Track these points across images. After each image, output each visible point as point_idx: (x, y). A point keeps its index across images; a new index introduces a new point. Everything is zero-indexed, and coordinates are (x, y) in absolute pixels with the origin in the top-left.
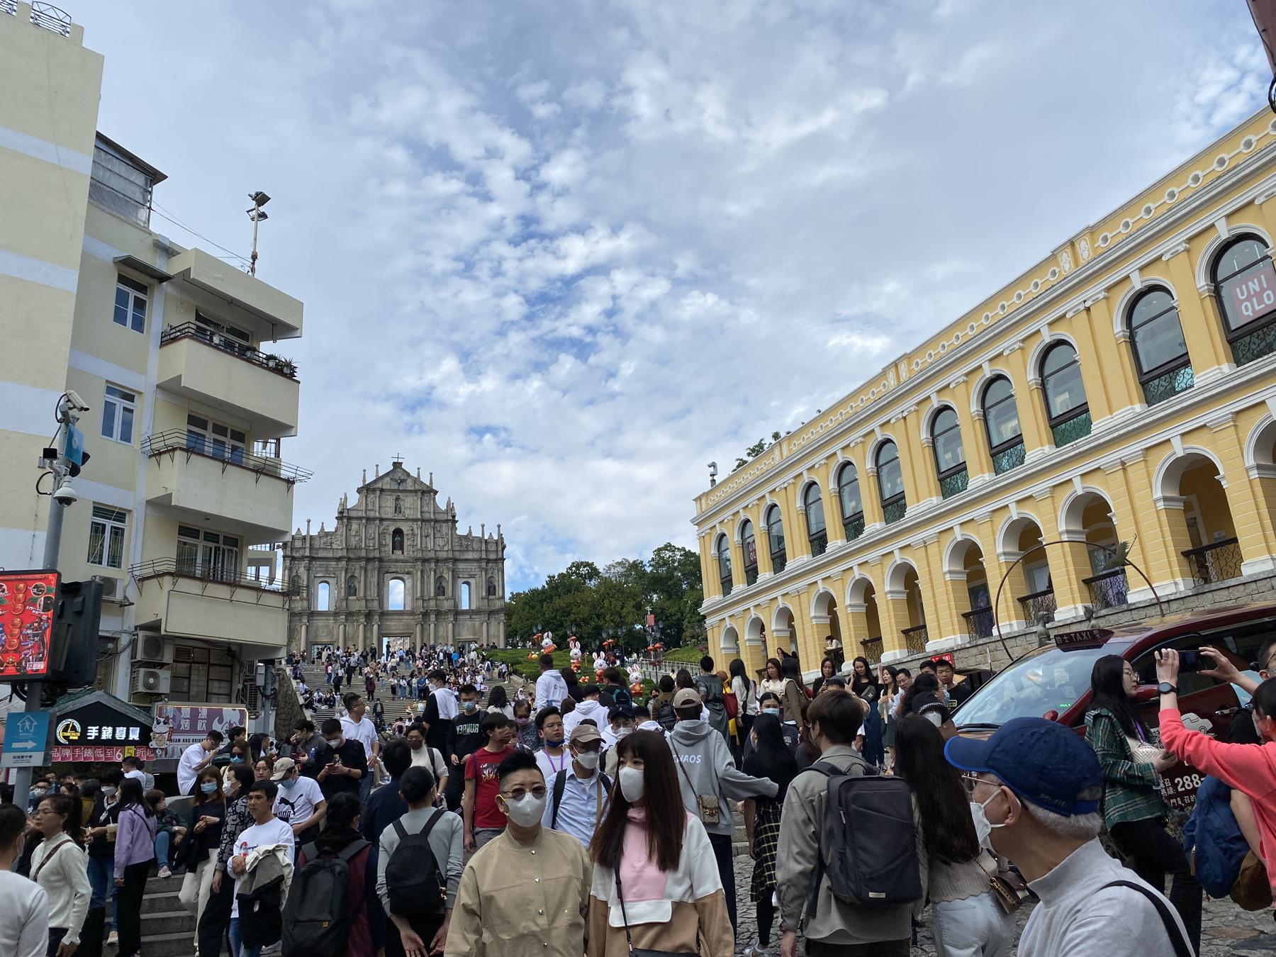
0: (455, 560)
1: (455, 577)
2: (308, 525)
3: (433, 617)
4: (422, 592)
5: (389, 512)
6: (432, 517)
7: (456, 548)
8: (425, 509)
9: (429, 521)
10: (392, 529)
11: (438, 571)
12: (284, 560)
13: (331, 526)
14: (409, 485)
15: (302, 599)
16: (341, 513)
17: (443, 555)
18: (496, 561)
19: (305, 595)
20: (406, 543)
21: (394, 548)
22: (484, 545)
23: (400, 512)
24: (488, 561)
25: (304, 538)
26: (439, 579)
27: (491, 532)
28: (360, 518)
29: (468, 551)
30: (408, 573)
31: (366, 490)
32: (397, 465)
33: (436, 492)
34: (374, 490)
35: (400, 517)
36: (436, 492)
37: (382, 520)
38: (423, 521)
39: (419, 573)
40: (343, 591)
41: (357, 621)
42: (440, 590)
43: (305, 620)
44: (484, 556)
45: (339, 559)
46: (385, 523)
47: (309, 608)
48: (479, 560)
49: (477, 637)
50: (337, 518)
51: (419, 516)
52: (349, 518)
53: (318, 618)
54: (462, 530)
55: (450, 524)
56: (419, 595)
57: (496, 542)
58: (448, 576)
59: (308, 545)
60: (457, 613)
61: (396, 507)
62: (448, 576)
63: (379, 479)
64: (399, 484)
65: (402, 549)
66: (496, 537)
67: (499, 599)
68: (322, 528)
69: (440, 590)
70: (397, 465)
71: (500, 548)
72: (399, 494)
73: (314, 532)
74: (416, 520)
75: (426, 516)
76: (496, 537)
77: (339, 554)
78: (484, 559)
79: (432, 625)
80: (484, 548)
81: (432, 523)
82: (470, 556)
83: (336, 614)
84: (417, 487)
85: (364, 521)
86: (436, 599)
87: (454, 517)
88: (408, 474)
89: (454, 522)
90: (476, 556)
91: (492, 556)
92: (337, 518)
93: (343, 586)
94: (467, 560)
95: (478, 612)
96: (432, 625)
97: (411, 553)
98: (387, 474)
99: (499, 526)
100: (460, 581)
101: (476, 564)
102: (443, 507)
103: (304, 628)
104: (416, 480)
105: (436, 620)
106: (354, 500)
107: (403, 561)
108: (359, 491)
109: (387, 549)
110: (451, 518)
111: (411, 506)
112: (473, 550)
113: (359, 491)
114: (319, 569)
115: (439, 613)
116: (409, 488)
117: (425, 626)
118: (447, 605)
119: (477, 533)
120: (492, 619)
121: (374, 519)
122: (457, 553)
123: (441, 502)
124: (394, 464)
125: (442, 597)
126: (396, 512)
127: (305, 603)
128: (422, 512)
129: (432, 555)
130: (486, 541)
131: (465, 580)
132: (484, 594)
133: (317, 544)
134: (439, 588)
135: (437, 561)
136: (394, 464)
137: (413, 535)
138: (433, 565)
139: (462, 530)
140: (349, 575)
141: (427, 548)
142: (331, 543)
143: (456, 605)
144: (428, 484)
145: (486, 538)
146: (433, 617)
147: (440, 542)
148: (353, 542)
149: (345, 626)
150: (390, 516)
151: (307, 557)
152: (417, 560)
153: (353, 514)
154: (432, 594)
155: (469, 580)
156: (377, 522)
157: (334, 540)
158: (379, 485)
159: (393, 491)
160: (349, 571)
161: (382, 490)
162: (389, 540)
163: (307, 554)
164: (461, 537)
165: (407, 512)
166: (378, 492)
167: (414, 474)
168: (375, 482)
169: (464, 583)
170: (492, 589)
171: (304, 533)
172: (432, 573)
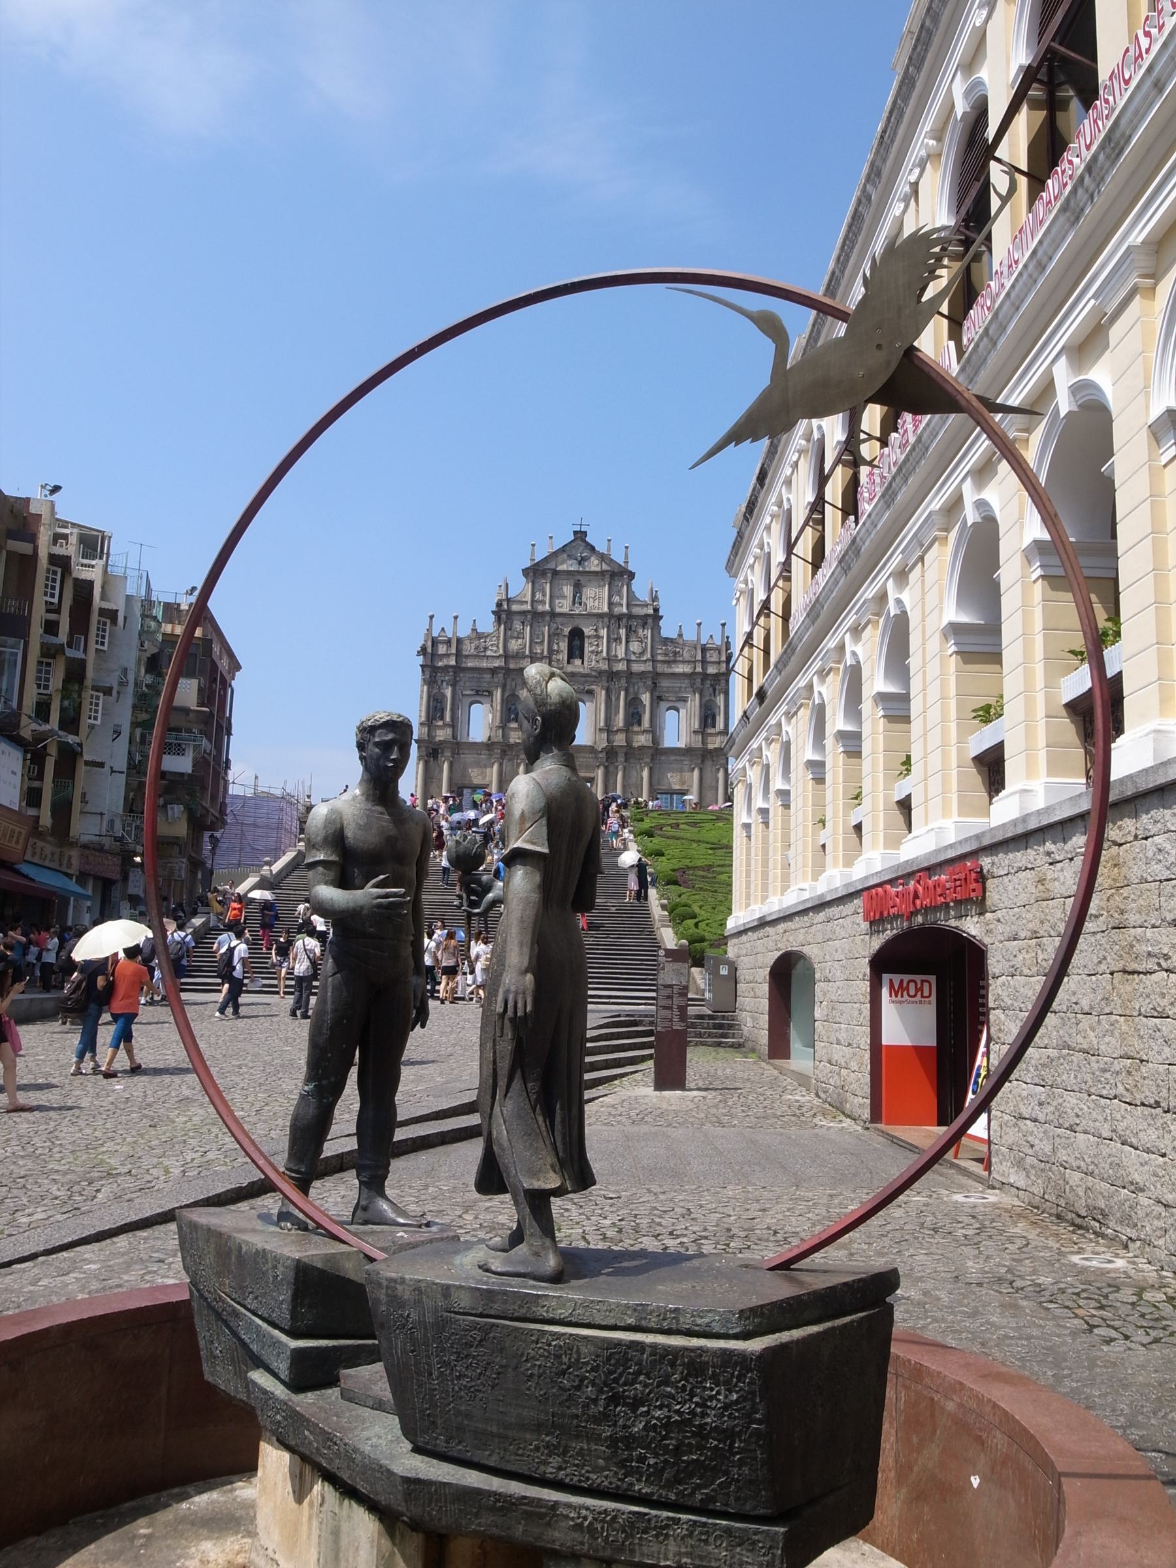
0: (656, 676)
1: (657, 699)
2: (455, 623)
3: (621, 759)
4: (608, 719)
5: (564, 606)
6: (625, 610)
7: (659, 658)
8: (616, 599)
9: (620, 618)
10: (567, 631)
11: (631, 690)
12: (423, 671)
13: (487, 624)
14: (594, 565)
15: (445, 725)
16: (499, 605)
17: (637, 668)
18: (717, 676)
19: (448, 719)
20: (587, 649)
21: (571, 657)
22: (699, 652)
23: (580, 604)
24: (705, 676)
25: (448, 642)
26: (634, 705)
27: (711, 635)
28: (524, 613)
29: (675, 662)
30: (590, 692)
31: (535, 572)
32: (580, 535)
33: (632, 575)
34: (544, 574)
35: (578, 610)
36: (632, 575)
37: (553, 615)
38: (610, 615)
39: (603, 692)
40: (498, 714)
41: (518, 756)
42: (634, 717)
43: (448, 754)
44: (699, 669)
45: (493, 671)
46: (559, 620)
47: (454, 737)
48: (691, 676)
49: (685, 787)
50: (493, 612)
51: (606, 609)
52: (510, 613)
53: (466, 752)
54: (668, 629)
55: (650, 621)
56: (602, 724)
57: (718, 650)
58: (646, 698)
59: (454, 651)
60: (657, 754)
61: (574, 597)
62: (646, 698)
63: (555, 555)
64: (580, 563)
65: (582, 657)
66: (718, 641)
67: (720, 733)
68: (474, 630)
69: (634, 717)
70: (580, 535)
71: (724, 658)
72: (581, 578)
73: (464, 631)
74: (600, 616)
75: (617, 610)
76: (718, 641)
77: (497, 663)
78: (699, 673)
79: (620, 767)
80: (699, 657)
81: (624, 620)
82: (680, 669)
83: (489, 746)
84: (605, 567)
85: (529, 617)
86: (627, 731)
87: (656, 610)
88: (593, 549)
89: (657, 617)
90: (687, 669)
91: (711, 670)
92: (493, 612)
93: (499, 708)
94: (674, 675)
95: (688, 751)
96: (620, 767)
97: (593, 663)
98: (563, 549)
99: (723, 625)
100: (664, 705)
101: (686, 681)
102: (643, 595)
103: (446, 766)
104: (603, 558)
105: (626, 761)
106: (520, 587)
107: (586, 675)
108: (526, 572)
109: (560, 657)
110: (651, 612)
111: (597, 598)
112: (684, 662)
113: (526, 572)
114: (468, 684)
115: (631, 753)
116: (593, 569)
117: (611, 769)
118: (642, 740)
119: (690, 636)
120: (709, 763)
121: (543, 614)
122: (659, 665)
123: (641, 590)
124: (575, 533)
125: (636, 728)
126: (574, 603)
127: (449, 731)
128: (610, 604)
129: (622, 666)
130: (704, 649)
131: (671, 704)
132: (697, 726)
133: (469, 648)
134: (633, 714)
135: (630, 675)
136: (575, 533)
137: (598, 637)
138: (623, 682)
139: (668, 629)
140: (507, 694)
141: (617, 656)
142: (486, 649)
143: (656, 741)
144: (623, 564)
145: (703, 642)
146: (621, 759)
147: (635, 647)
148: (514, 645)
149: (501, 765)
150: (565, 610)
151: (452, 667)
152: (601, 673)
153: (515, 608)
154: (621, 724)
155: (677, 704)
156: (548, 618)
157: (488, 644)
158: (552, 565)
159: (569, 573)
160: (508, 687)
161: (555, 573)
162: (564, 646)
163: (453, 663)
164: (667, 641)
165: (590, 603)
166: (549, 575)
167: (601, 548)
168: (546, 560)
169: (668, 709)
170: (710, 721)
171: (450, 635)
172: (623, 693)
